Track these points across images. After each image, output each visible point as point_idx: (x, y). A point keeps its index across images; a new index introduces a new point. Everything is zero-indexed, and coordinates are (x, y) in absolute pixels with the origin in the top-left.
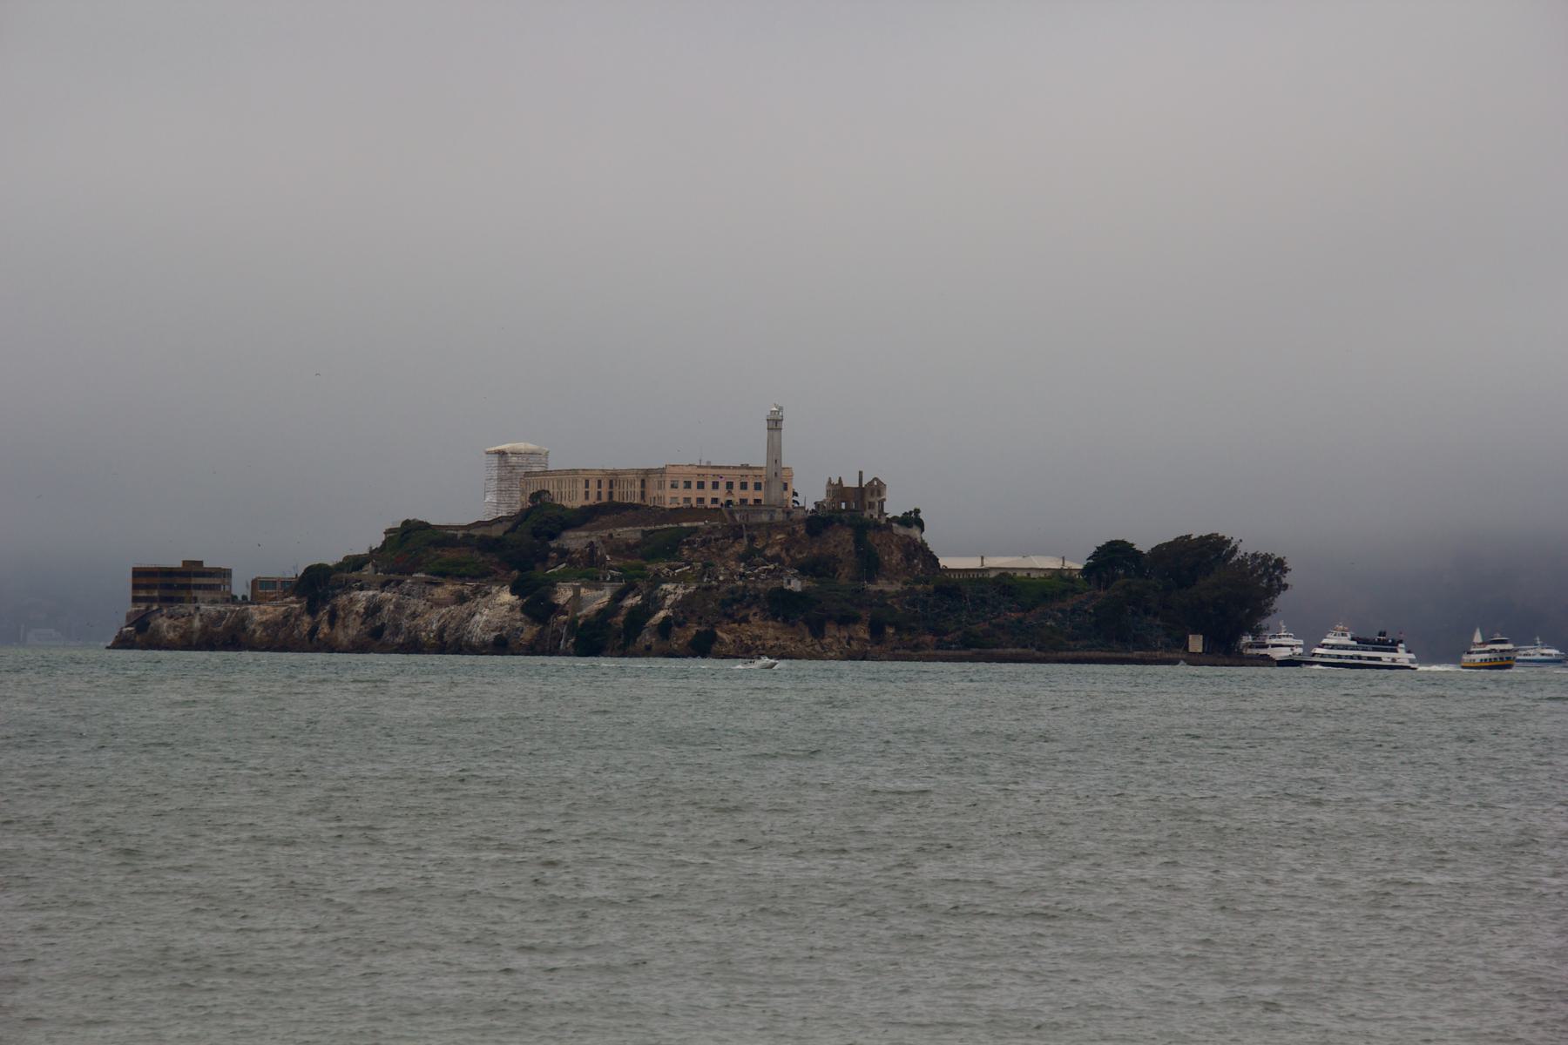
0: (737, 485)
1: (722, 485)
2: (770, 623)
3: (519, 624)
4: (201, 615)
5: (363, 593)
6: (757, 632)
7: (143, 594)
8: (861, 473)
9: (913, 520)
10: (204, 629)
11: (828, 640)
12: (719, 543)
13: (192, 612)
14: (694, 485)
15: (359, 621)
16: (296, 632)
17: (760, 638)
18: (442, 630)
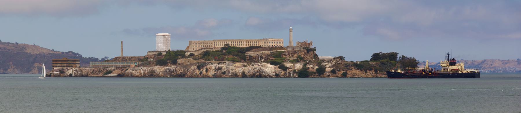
0: (277, 43)
1: (275, 43)
2: (357, 70)
3: (280, 71)
4: (143, 70)
5: (213, 65)
6: (355, 72)
7: (54, 65)
8: (307, 40)
9: (314, 49)
10: (144, 73)
11: (368, 74)
12: (292, 54)
13: (140, 69)
14: (272, 42)
15: (214, 71)
16: (194, 73)
17: (355, 73)
18: (243, 73)
